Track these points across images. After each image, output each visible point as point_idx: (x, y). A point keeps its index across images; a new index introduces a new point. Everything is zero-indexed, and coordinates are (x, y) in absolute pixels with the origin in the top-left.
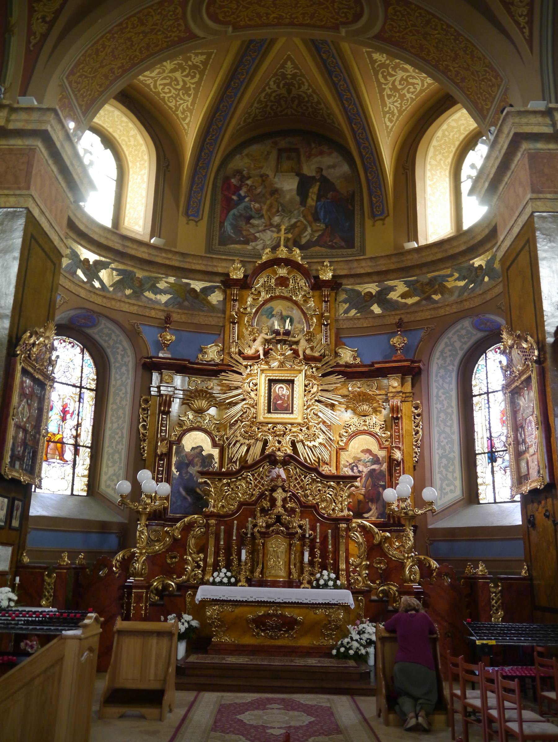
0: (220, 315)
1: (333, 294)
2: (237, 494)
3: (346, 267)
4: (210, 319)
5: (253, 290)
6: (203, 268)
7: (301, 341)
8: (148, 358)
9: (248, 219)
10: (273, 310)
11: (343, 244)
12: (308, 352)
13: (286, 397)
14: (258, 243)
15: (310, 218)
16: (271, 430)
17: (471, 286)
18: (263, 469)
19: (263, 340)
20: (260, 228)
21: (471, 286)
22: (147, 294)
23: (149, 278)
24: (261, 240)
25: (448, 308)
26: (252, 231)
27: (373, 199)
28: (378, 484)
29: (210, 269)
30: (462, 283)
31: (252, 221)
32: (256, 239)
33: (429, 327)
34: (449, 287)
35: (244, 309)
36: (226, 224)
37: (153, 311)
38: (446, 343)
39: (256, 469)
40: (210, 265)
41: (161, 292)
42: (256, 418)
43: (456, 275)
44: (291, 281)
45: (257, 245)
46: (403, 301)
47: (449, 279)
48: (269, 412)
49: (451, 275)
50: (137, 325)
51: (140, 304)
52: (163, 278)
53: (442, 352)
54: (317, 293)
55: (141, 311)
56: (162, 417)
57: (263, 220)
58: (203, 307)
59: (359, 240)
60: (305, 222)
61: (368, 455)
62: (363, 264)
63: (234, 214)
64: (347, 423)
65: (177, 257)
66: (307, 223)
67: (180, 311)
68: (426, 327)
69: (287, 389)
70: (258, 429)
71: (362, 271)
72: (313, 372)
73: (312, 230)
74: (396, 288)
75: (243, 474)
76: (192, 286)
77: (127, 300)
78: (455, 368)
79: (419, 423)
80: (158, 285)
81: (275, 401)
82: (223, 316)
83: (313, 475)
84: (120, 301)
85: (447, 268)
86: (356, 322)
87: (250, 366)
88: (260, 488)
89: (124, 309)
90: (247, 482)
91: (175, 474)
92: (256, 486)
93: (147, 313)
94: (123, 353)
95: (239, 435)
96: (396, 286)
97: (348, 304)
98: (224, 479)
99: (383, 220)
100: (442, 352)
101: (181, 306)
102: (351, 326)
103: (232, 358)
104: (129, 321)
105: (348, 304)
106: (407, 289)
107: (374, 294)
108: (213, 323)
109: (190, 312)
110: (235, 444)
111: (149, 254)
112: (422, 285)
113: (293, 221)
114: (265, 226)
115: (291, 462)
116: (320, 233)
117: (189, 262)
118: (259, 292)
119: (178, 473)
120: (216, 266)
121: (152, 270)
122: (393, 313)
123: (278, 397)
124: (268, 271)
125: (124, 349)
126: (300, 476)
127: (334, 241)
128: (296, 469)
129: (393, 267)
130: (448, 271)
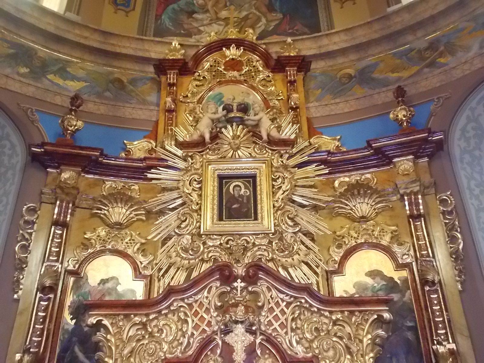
0: (152, 108)
1: (301, 76)
2: (160, 344)
3: (314, 46)
4: (140, 112)
5: (197, 74)
6: (131, 52)
7: (262, 120)
8: (38, 146)
9: (191, 14)
10: (223, 97)
11: (306, 30)
12: (274, 133)
13: (245, 198)
14: (202, 36)
15: (264, 9)
16: (225, 245)
18: (209, 292)
19: (210, 121)
20: (205, 22)
22: (50, 77)
23: (58, 60)
24: (206, 33)
25: (466, 67)
26: (195, 24)
28: (403, 325)
29: (140, 54)
31: (195, 16)
32: (200, 32)
33: (441, 97)
35: (184, 97)
36: (163, 17)
37: (58, 97)
38: (468, 117)
39: (195, 294)
40: (140, 50)
41: (74, 78)
42: (200, 227)
44: (245, 64)
45: (201, 38)
46: (395, 75)
48: (220, 219)
50: (32, 111)
51: (39, 85)
52: (78, 63)
53: (464, 130)
54: (279, 77)
55: (39, 95)
56: (54, 232)
57: (208, 15)
58: (130, 100)
59: (325, 24)
60: (258, 13)
61: (378, 279)
62: (336, 39)
63: (174, 9)
64: (338, 233)
65: (96, 36)
66: (260, 15)
67: (97, 100)
68: (436, 97)
69: (246, 187)
70: (204, 243)
71: (336, 48)
72: (282, 162)
73: (267, 20)
75: (171, 304)
76: (116, 76)
77: (17, 77)
79: (454, 224)
80: (68, 69)
81: (228, 205)
82: (156, 108)
83: (303, 301)
84: (7, 76)
86: (333, 107)
87: (191, 157)
88: (204, 331)
89: (13, 89)
90: (179, 318)
91: (68, 324)
92: (196, 327)
93: (49, 98)
94: (10, 152)
95: (174, 254)
97: (320, 90)
98: (135, 315)
100: (464, 130)
101: (99, 95)
102: (327, 113)
103: (167, 150)
104: (18, 104)
105: (320, 90)
108: (143, 117)
109: (112, 103)
110: (166, 271)
111: (57, 28)
112: (419, 51)
113: (244, 13)
114: (211, 20)
115: (261, 279)
116: (277, 22)
117: (113, 45)
118: (204, 77)
119: (74, 321)
120: (147, 51)
121: (61, 51)
122: (384, 89)
123: (233, 199)
124: (215, 56)
125: (13, 147)
126: (277, 304)
127: (295, 28)
128: (269, 290)
129: (376, 36)
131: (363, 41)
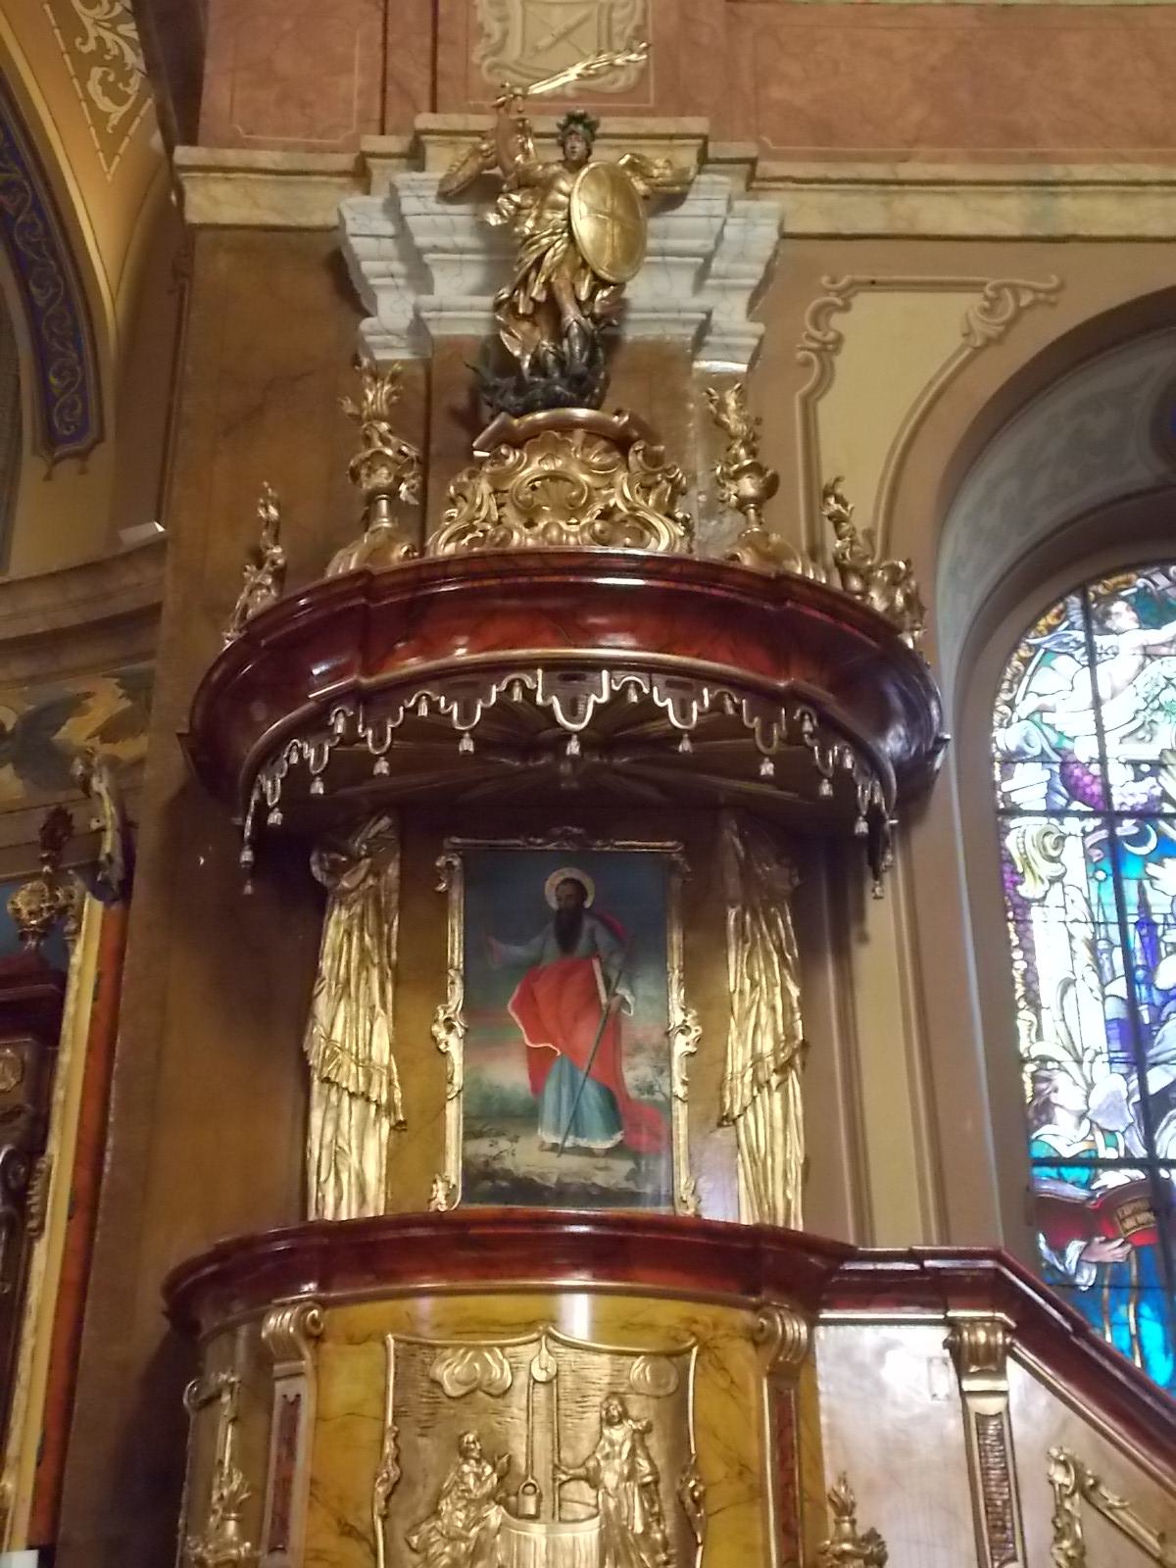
27: (53, 380)
74: (90, 702)
96: (88, 695)
99: (83, 455)
106: (127, 704)
107: (9, 728)
129: (71, 618)
131: (39, 630)
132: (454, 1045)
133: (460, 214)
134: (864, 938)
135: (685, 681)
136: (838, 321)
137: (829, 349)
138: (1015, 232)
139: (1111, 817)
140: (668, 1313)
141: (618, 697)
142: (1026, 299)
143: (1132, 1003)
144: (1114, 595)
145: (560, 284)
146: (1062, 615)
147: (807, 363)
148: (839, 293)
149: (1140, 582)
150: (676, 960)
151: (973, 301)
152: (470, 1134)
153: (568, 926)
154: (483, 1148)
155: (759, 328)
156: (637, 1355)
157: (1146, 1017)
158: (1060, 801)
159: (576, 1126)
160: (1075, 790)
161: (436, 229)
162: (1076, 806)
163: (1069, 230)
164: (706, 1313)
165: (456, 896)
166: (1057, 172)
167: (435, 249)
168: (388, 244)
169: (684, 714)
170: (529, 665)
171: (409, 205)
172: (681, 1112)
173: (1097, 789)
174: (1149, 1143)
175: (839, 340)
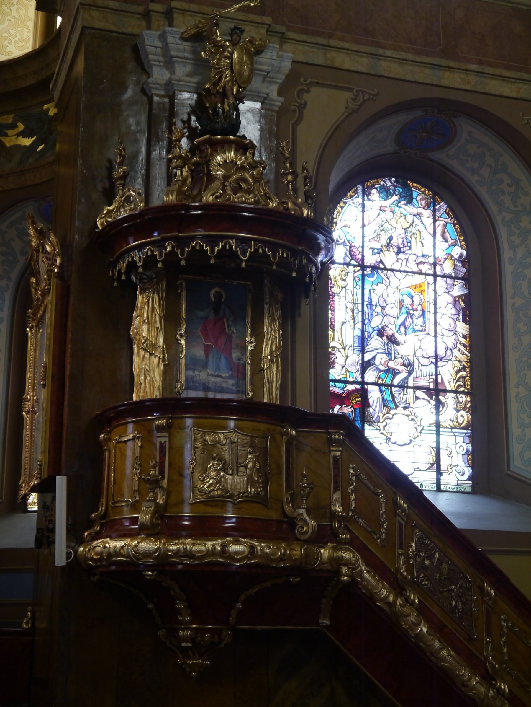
17: (40, 148)
21: (40, 148)
30: (27, 142)
34: (8, 145)
43: (21, 127)
47: (10, 132)
49: (14, 126)
78: (12, 285)
85: (9, 113)
130: (9, 119)
132: (183, 342)
133: (187, 45)
134: (300, 315)
135: (274, 248)
136: (305, 96)
137: (303, 106)
138: (364, 70)
139: (363, 267)
140: (263, 427)
141: (256, 250)
142: (367, 97)
143: (363, 331)
144: (373, 187)
145: (228, 87)
146: (356, 192)
147: (295, 111)
148: (307, 85)
149: (382, 183)
150: (249, 320)
151: (348, 95)
152: (187, 369)
153: (217, 307)
154: (190, 373)
155: (282, 99)
156: (256, 437)
157: (366, 336)
158: (348, 260)
159: (218, 368)
160: (353, 257)
161: (178, 50)
162: (353, 262)
163: (382, 73)
164: (272, 427)
165: (184, 293)
166: (381, 51)
167: (178, 57)
168: (159, 50)
169: (274, 257)
170: (232, 237)
171: (170, 39)
172: (249, 368)
173: (360, 257)
174: (363, 377)
175: (305, 104)
